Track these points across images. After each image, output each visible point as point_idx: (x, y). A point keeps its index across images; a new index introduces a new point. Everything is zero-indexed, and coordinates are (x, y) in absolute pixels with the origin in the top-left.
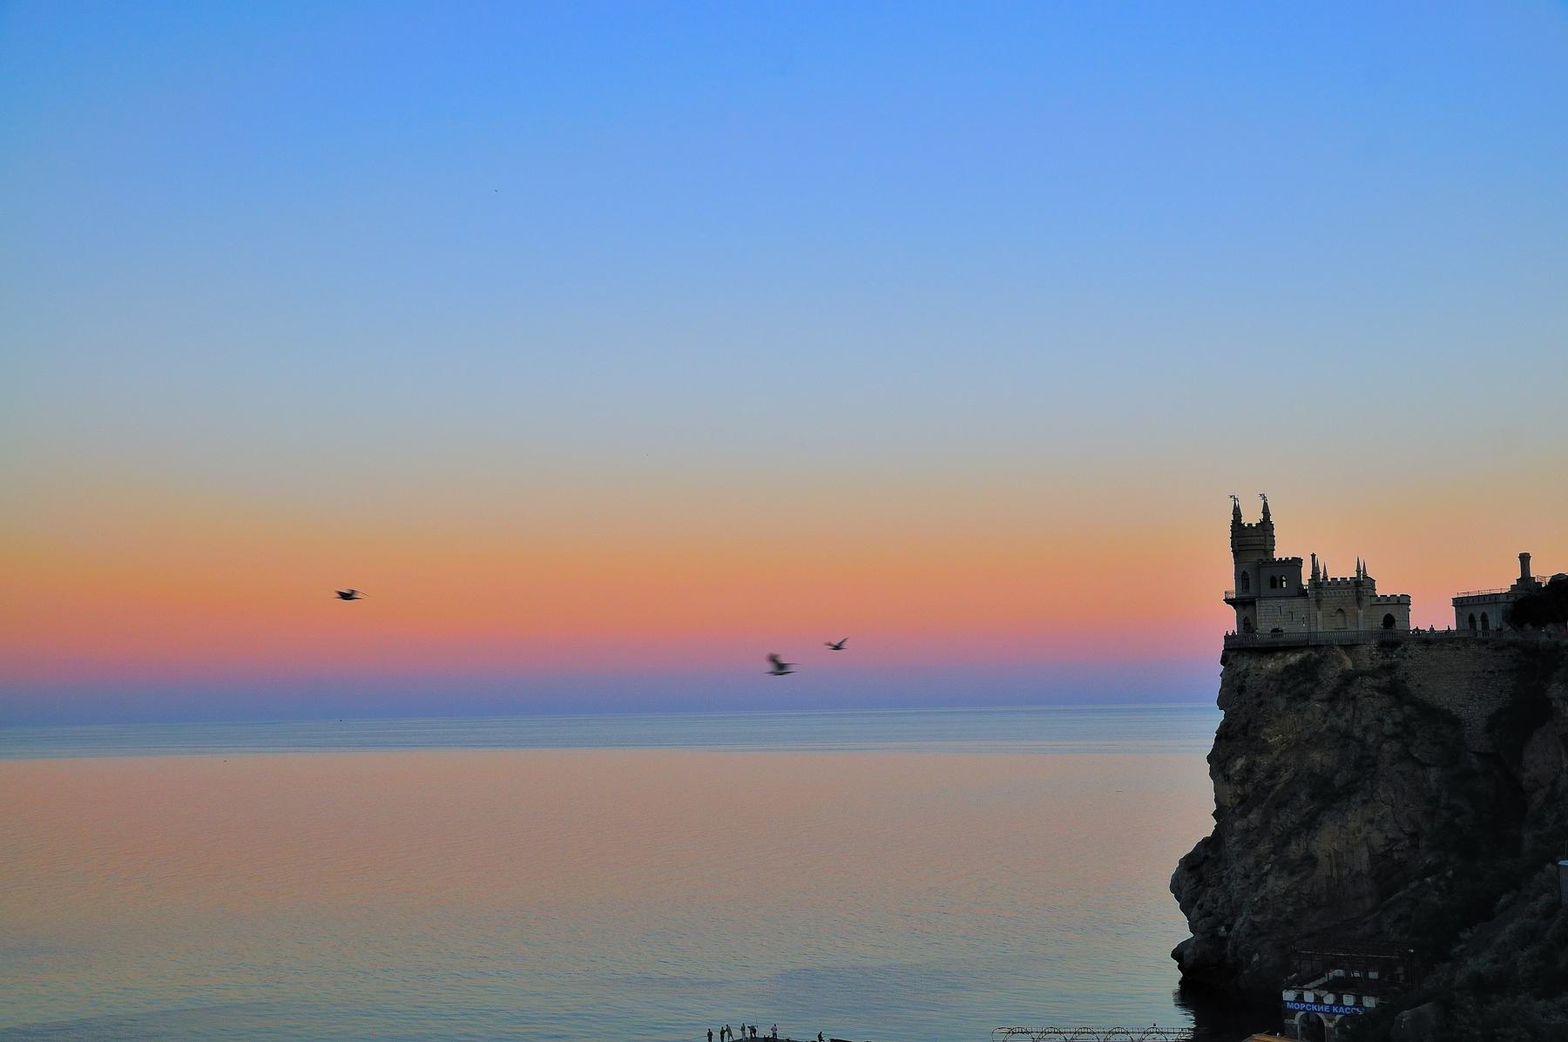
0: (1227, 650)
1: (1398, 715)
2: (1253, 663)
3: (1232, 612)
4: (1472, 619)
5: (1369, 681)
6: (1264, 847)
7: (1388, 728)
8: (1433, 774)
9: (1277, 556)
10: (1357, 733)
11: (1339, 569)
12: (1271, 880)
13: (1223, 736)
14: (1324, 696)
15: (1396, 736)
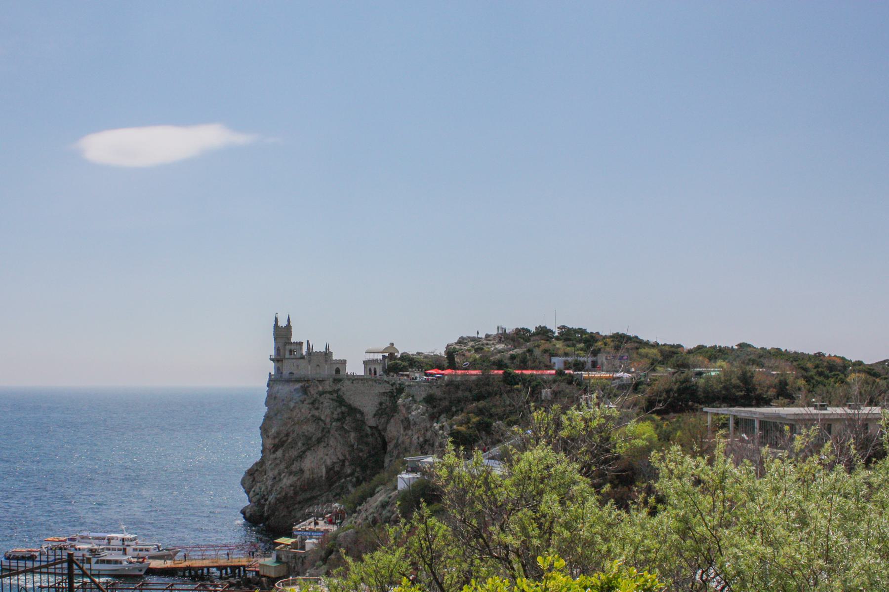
0: (270, 380)
1: (339, 410)
2: (280, 387)
3: (272, 364)
4: (370, 370)
5: (328, 396)
6: (282, 467)
7: (335, 416)
8: (353, 435)
9: (292, 341)
10: (323, 418)
11: (319, 348)
12: (285, 480)
13: (267, 417)
14: (311, 401)
15: (338, 420)
